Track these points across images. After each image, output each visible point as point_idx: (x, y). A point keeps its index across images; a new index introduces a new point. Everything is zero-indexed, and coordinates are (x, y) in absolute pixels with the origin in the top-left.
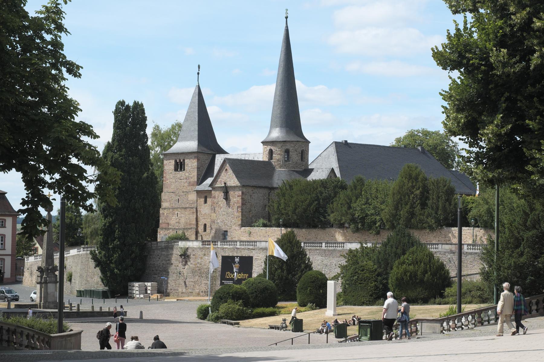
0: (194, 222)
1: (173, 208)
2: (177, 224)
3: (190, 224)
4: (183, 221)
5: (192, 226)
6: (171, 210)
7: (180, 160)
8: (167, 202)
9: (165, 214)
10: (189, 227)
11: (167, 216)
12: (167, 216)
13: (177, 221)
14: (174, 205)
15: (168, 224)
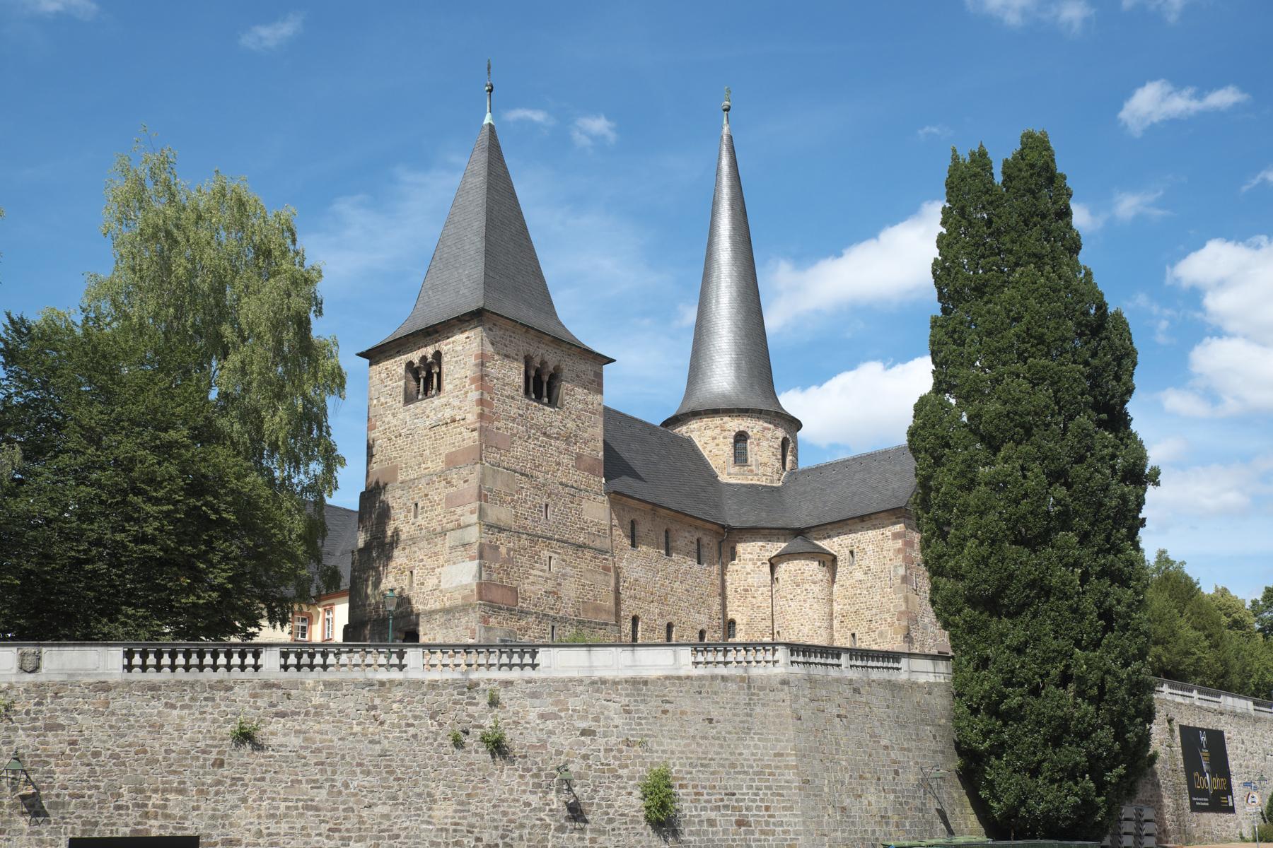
0: (610, 603)
1: (534, 538)
2: (551, 600)
3: (598, 609)
4: (570, 590)
5: (603, 617)
6: (525, 541)
7: (543, 363)
8: (502, 502)
9: (503, 550)
10: (591, 616)
11: (510, 560)
12: (510, 560)
13: (549, 586)
14: (529, 524)
15: (514, 590)
